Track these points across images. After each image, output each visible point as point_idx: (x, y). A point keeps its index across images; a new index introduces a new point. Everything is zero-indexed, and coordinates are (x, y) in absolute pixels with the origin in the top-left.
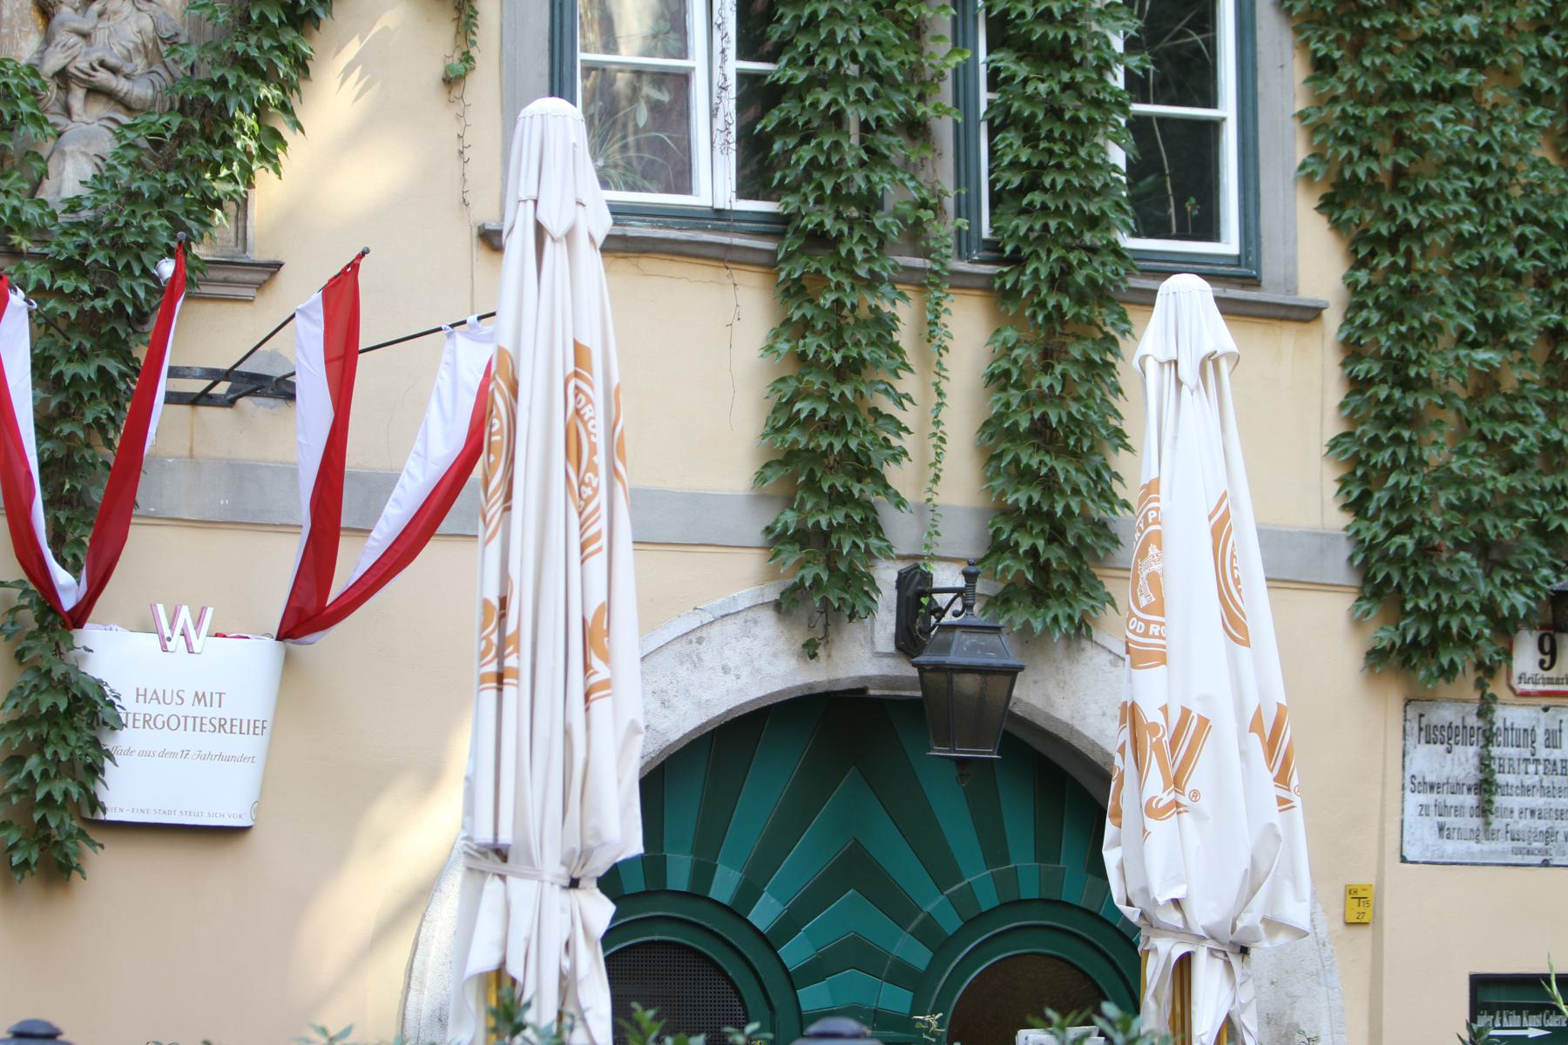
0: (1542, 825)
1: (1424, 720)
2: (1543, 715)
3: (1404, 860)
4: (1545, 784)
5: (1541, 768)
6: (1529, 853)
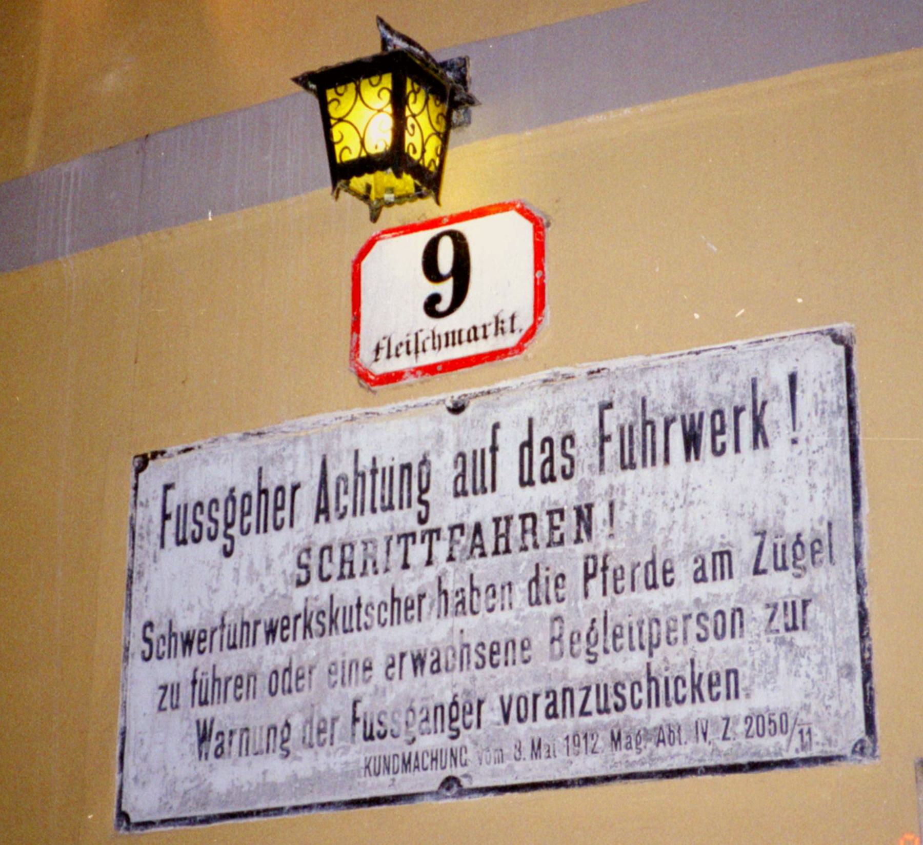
0: (442, 688)
1: (175, 498)
4: (450, 585)
5: (441, 549)
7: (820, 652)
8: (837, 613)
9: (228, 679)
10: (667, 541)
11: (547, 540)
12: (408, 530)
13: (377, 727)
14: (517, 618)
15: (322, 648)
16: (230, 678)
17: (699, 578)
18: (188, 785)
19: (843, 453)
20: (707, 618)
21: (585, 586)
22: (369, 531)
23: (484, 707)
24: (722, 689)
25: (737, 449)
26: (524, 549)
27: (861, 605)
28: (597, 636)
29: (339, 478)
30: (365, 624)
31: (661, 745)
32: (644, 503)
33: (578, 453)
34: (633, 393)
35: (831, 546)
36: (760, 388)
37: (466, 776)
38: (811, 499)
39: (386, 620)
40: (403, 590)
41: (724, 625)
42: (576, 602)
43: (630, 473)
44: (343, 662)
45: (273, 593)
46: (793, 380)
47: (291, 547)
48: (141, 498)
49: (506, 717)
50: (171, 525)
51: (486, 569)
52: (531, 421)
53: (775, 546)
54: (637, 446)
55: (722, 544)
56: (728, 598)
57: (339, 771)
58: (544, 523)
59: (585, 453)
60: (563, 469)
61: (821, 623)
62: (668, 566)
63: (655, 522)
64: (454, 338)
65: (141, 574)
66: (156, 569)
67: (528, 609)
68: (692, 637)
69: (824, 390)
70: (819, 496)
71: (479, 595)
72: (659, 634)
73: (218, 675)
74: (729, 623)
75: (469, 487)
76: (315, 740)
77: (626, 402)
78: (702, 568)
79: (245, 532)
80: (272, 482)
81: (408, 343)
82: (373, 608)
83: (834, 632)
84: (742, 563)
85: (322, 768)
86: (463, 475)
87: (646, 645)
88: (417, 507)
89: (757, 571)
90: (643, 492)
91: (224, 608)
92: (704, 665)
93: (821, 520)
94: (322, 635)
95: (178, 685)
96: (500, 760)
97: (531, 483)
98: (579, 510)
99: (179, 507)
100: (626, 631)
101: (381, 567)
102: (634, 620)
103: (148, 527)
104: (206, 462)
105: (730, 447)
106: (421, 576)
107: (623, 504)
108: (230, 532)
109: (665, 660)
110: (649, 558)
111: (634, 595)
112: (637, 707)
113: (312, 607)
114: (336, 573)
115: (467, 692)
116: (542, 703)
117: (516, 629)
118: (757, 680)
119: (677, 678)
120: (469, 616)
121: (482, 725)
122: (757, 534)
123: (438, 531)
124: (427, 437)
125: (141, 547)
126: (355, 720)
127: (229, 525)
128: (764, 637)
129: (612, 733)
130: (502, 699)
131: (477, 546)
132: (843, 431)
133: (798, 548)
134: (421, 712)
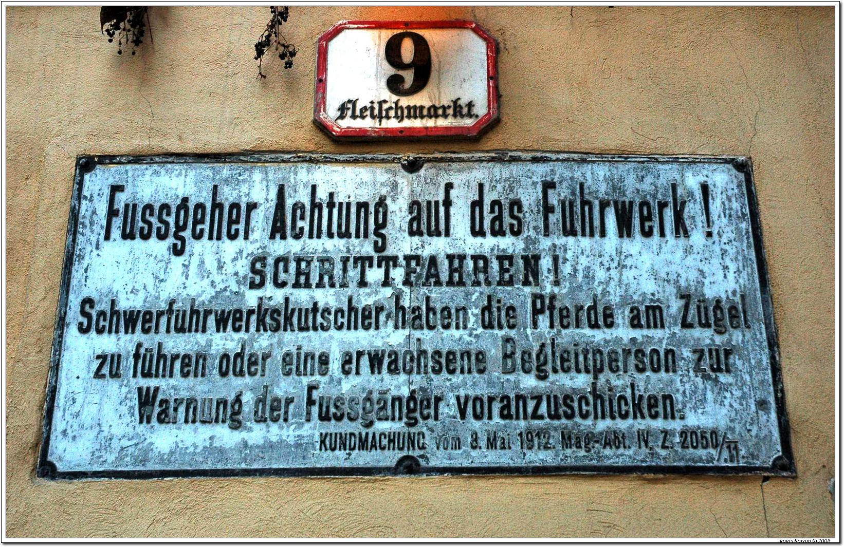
0: (399, 385)
1: (122, 199)
2: (404, 180)
3: (47, 470)
4: (406, 302)
5: (398, 274)
6: (363, 444)
7: (741, 388)
8: (753, 362)
9: (175, 357)
10: (605, 293)
11: (498, 279)
12: (364, 254)
13: (333, 410)
14: (470, 335)
15: (275, 340)
16: (177, 356)
17: (635, 323)
18: (125, 443)
19: (749, 247)
20: (644, 355)
21: (534, 318)
22: (325, 251)
23: (441, 405)
24: (660, 409)
25: (662, 234)
26: (478, 283)
27: (773, 358)
28: (546, 357)
29: (295, 205)
30: (322, 324)
31: (608, 448)
32: (584, 261)
33: (524, 217)
34: (572, 178)
35: (745, 312)
36: (680, 191)
37: (422, 456)
38: (725, 277)
39: (342, 323)
40: (359, 301)
41: (659, 360)
42: (525, 328)
43: (571, 240)
44: (298, 355)
45: (225, 289)
46: (705, 188)
47: (244, 255)
48: (86, 192)
49: (463, 415)
50: (117, 222)
51: (441, 295)
52: (481, 186)
53: (699, 307)
54: (578, 217)
55: (652, 300)
56: (660, 341)
57: (292, 443)
58: (495, 265)
59: (532, 219)
60: (512, 226)
61: (740, 367)
62: (608, 312)
63: (593, 277)
64: (416, 112)
65: (81, 257)
66: (98, 255)
67: (480, 330)
68: (631, 367)
69: (730, 200)
70: (731, 276)
71: (435, 314)
72: (602, 361)
73: (165, 351)
74: (666, 361)
75: (424, 228)
76: (267, 415)
77: (565, 184)
78: (637, 317)
79: (198, 236)
80: (227, 199)
81: (372, 108)
82: (329, 313)
83: (751, 376)
84: (670, 316)
85: (274, 439)
86: (417, 219)
87: (591, 368)
88: (372, 237)
89: (686, 325)
90: (582, 253)
91: (173, 295)
92: (642, 389)
93: (734, 293)
94: (276, 329)
95: (119, 356)
96: (458, 444)
97: (482, 233)
98: (525, 258)
99: (127, 206)
100: (573, 356)
101: (337, 280)
102: (580, 348)
103: (91, 217)
104: (156, 173)
105: (656, 230)
106: (377, 293)
107: (565, 260)
108: (182, 234)
109: (607, 381)
110: (589, 303)
111: (578, 331)
112: (585, 416)
113: (267, 304)
114: (292, 280)
115: (421, 389)
116: (496, 407)
117: (470, 343)
118: (688, 405)
119: (621, 397)
120: (426, 331)
121: (440, 417)
122: (682, 297)
123: (395, 259)
124: (382, 184)
125: (83, 234)
126: (310, 402)
127: (180, 228)
128: (692, 373)
129: (562, 433)
130: (458, 398)
131: (433, 276)
132: (747, 232)
133: (719, 312)
134: (378, 403)
